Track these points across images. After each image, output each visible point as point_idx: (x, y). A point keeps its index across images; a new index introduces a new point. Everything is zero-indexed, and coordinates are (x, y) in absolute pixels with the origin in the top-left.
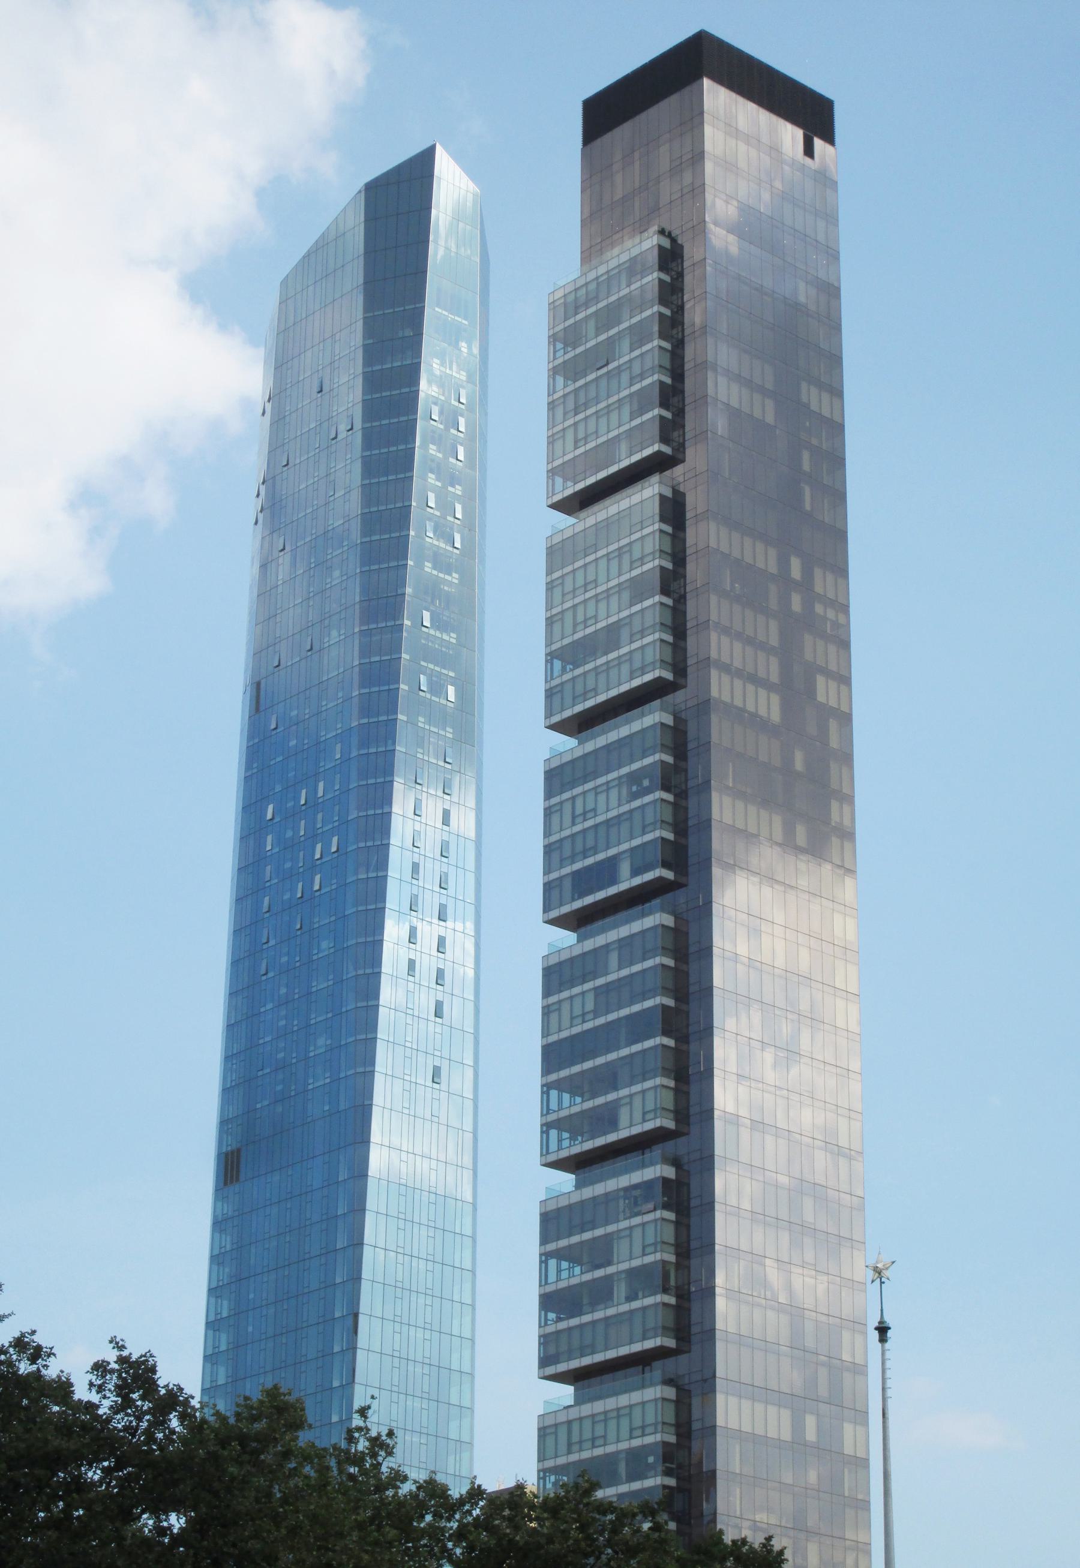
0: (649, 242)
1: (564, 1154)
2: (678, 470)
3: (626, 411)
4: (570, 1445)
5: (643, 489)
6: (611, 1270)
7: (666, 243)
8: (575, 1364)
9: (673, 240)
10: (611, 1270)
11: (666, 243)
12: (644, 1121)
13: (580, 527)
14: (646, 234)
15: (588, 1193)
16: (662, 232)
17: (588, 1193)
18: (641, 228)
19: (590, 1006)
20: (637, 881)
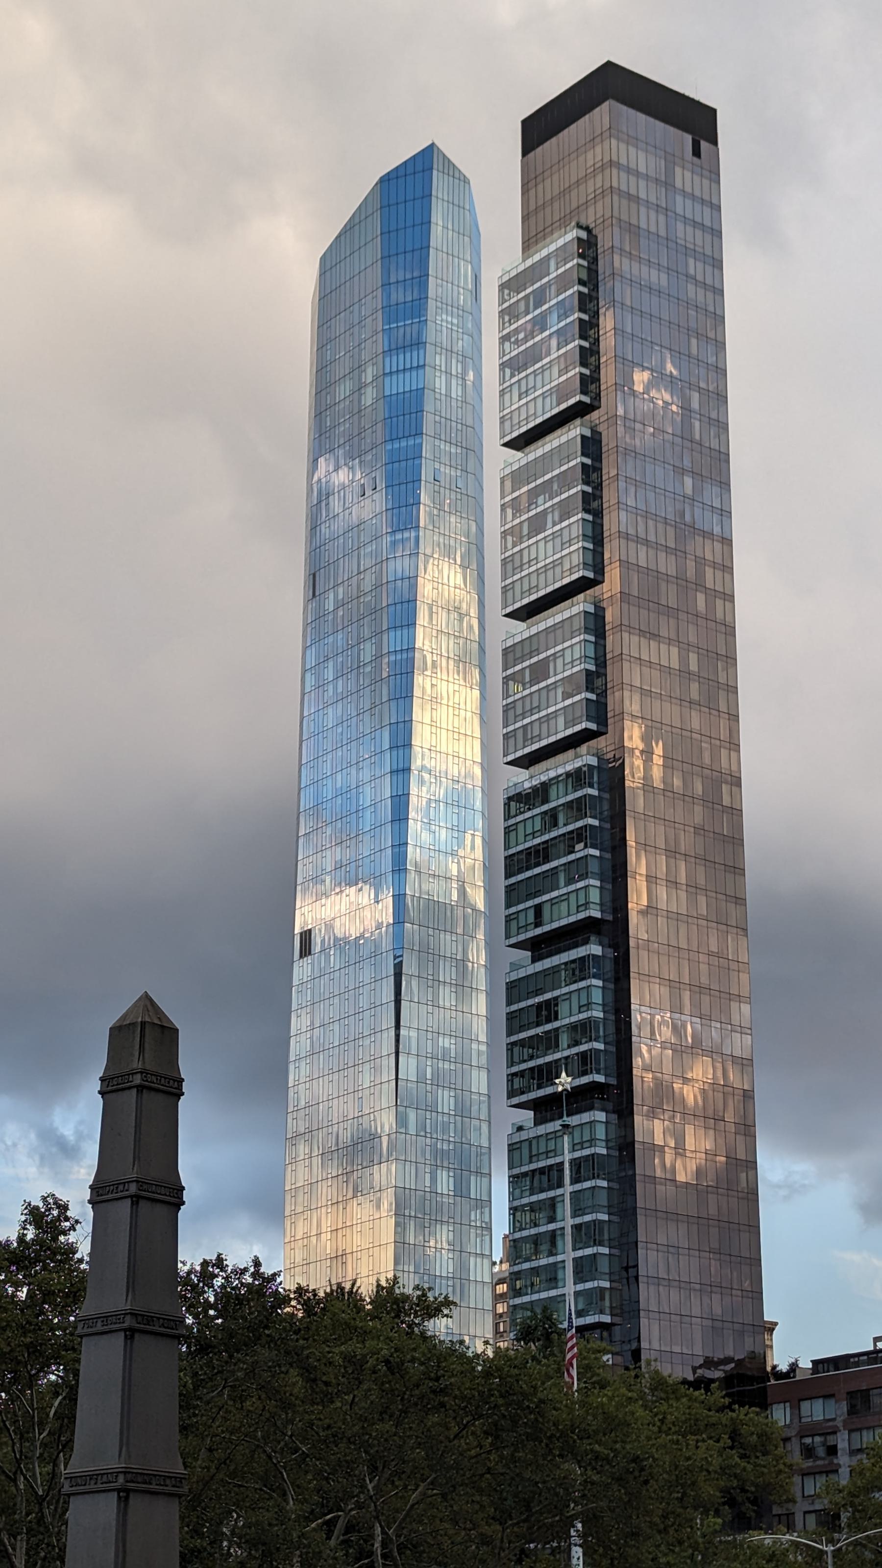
0: (573, 234)
1: (522, 937)
2: (595, 415)
3: (555, 370)
4: (531, 1157)
5: (569, 430)
6: (556, 1024)
7: (583, 235)
8: (532, 1095)
9: (588, 229)
10: (556, 1024)
11: (583, 235)
12: (578, 912)
13: (524, 462)
14: (568, 228)
15: (539, 966)
16: (579, 226)
17: (539, 966)
18: (563, 223)
19: (538, 827)
20: (569, 732)
